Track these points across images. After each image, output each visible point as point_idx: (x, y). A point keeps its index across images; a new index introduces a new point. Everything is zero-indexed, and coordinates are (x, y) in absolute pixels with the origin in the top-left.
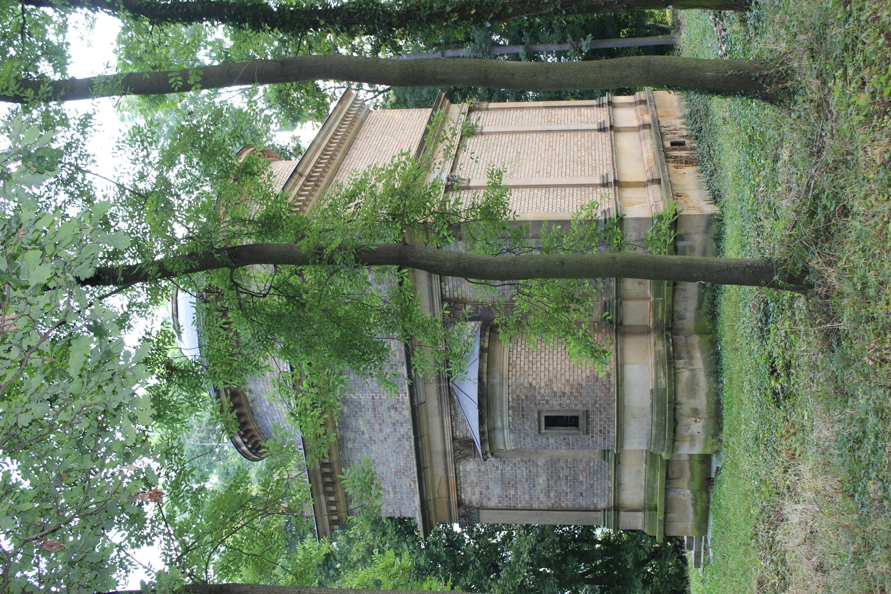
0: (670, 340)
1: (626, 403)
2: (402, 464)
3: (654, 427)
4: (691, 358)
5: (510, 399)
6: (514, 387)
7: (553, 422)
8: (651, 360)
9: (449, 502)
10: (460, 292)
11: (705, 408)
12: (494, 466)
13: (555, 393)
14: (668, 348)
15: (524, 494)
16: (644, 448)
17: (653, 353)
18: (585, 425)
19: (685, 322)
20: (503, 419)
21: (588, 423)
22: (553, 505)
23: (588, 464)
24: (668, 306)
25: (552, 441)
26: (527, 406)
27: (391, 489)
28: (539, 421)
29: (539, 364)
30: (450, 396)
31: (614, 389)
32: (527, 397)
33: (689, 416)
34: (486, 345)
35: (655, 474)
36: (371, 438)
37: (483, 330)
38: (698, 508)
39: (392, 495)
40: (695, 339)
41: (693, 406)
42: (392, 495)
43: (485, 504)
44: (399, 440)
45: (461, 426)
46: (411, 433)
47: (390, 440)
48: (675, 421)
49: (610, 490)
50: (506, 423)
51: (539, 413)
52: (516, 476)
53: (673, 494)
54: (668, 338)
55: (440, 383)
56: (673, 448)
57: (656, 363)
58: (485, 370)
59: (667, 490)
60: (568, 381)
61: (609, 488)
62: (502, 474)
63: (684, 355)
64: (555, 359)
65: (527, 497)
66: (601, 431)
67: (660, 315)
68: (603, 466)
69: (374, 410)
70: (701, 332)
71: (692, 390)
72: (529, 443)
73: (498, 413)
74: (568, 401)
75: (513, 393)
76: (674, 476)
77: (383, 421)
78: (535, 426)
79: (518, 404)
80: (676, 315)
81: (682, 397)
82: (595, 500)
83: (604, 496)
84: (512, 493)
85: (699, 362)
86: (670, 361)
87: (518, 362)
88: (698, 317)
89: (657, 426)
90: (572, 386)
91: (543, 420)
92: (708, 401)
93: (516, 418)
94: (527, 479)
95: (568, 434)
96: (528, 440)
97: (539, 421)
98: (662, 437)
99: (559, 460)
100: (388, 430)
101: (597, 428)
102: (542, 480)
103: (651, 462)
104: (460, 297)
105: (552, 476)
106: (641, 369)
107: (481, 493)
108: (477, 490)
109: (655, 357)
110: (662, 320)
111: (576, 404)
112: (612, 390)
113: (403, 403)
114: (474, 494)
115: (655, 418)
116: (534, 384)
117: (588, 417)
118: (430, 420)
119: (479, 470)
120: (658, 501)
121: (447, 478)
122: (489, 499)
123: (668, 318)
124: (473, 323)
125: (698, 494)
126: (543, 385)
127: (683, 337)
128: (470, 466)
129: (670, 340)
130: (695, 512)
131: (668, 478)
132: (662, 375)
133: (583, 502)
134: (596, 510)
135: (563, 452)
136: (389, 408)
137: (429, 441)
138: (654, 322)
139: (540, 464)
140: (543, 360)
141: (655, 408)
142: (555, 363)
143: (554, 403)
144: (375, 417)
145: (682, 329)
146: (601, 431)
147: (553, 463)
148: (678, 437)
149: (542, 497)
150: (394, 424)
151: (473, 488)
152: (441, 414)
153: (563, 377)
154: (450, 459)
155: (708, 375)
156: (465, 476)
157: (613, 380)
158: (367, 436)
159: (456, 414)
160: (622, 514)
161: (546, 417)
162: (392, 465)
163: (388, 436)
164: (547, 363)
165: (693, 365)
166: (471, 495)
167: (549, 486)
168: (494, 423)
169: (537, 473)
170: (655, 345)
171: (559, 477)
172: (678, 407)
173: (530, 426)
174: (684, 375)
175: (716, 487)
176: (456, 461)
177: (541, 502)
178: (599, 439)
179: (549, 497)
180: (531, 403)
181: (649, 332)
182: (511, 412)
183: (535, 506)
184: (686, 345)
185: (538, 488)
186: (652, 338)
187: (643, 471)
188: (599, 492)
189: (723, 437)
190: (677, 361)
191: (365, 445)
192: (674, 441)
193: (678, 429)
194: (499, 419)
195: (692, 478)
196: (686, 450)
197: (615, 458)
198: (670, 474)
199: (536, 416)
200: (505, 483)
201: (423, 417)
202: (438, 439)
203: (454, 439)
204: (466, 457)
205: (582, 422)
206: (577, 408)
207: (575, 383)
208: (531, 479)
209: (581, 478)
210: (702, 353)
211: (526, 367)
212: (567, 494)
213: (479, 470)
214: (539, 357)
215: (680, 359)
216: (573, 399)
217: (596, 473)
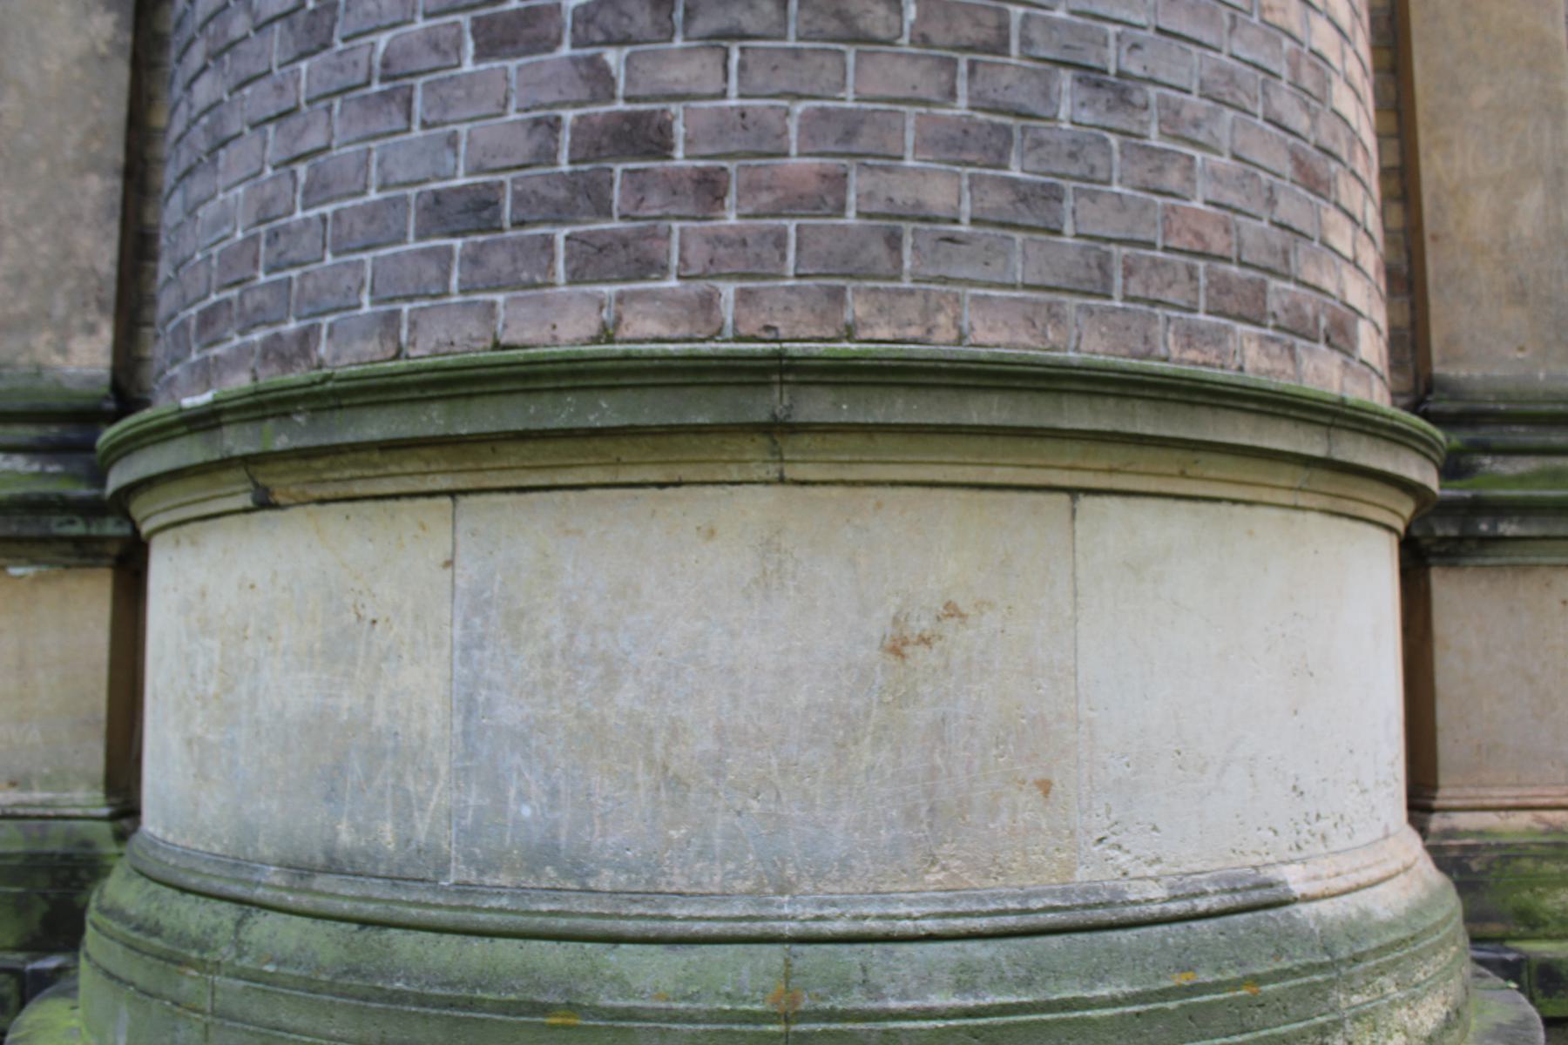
3: (746, 977)
66: (643, 136)
110: (1532, 923)
115: (922, 985)
146: (643, 136)
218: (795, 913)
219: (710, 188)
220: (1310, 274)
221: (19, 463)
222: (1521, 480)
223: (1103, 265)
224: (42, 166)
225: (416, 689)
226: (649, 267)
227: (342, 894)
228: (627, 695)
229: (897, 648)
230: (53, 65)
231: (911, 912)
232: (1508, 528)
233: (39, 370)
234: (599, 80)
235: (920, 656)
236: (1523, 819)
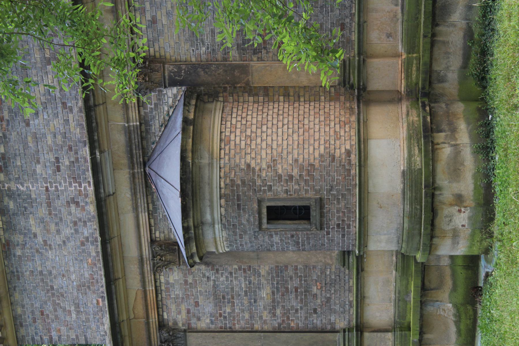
0: (428, 108)
1: (371, 189)
2: (87, 275)
3: (406, 220)
4: (454, 130)
5: (223, 185)
6: (227, 170)
7: (277, 214)
8: (403, 133)
9: (148, 324)
10: (157, 49)
11: (471, 193)
12: (204, 276)
13: (280, 177)
14: (424, 118)
15: (243, 311)
16: (394, 247)
17: (405, 125)
18: (318, 217)
19: (446, 85)
20: (213, 210)
21: (322, 215)
22: (280, 325)
23: (323, 272)
24: (425, 64)
25: (276, 239)
26: (244, 193)
27: (73, 308)
28: (260, 213)
29: (259, 140)
30: (147, 186)
31: (355, 171)
32: (243, 182)
33: (451, 205)
34: (191, 116)
35: (408, 284)
36: (45, 241)
37: (187, 97)
38: (462, 327)
39: (74, 316)
40: (459, 107)
41: (456, 191)
42: (74, 316)
43: (193, 326)
44: (83, 244)
45: (162, 225)
46: (97, 234)
47: (70, 244)
48: (433, 212)
49: (351, 306)
50: (217, 216)
51: (260, 202)
52: (232, 289)
53: (430, 309)
54: (424, 106)
55: (133, 168)
56: (430, 248)
57: (410, 138)
58: (190, 147)
59: (422, 304)
60: (296, 161)
61: (351, 303)
62: (215, 287)
63: (444, 126)
64: (280, 133)
65: (247, 316)
66: (338, 225)
67: (414, 76)
68: (342, 275)
69: (49, 205)
70: (465, 98)
71: (456, 172)
72: (246, 242)
73: (207, 203)
74: (297, 187)
75: (226, 176)
76: (432, 286)
77: (61, 219)
78: (254, 219)
79: (233, 191)
80: (434, 76)
81: (442, 179)
82: (333, 319)
83: (344, 312)
84: (228, 310)
85: (464, 136)
86: (427, 136)
87: (233, 137)
88: (463, 78)
89: (410, 217)
90: (301, 168)
91: (264, 211)
92: (475, 184)
93: (230, 210)
94: (246, 292)
95: (297, 230)
96: (246, 238)
97: (260, 213)
98: (416, 232)
99: (286, 267)
100: (67, 231)
101: (334, 222)
102: (265, 293)
103: (403, 268)
104: (157, 55)
105: (277, 288)
106: (390, 147)
107: (188, 312)
108: (183, 308)
109: (408, 129)
110: (417, 84)
111: (307, 191)
112: (353, 172)
113: (86, 196)
114: (179, 313)
115: (407, 208)
116: (253, 165)
117: (322, 207)
118: (122, 218)
119: (186, 282)
120: (412, 318)
121: (145, 292)
122: (199, 319)
123: (424, 80)
124: (175, 90)
125: (462, 309)
126: (264, 166)
127: (443, 105)
128: (173, 277)
129: (428, 108)
130: (459, 332)
131: (424, 289)
132: (417, 152)
133: (317, 321)
134: (334, 331)
135: (291, 256)
136: (68, 203)
137: (121, 245)
138: (407, 86)
139: (263, 272)
140: (264, 135)
141: (408, 194)
142: (280, 138)
143: (279, 189)
144: (50, 214)
145: (443, 95)
146: (338, 225)
147: (279, 270)
148: (437, 232)
149: (266, 315)
150: (75, 223)
151: (178, 305)
152: (136, 209)
153: (290, 156)
154: (147, 268)
155: (476, 152)
156: (167, 290)
157: (354, 158)
158: (40, 239)
159: (155, 209)
160: (366, 335)
161: (269, 208)
162: (73, 277)
163: (68, 239)
164: (269, 138)
165: (456, 139)
166: (176, 314)
167: (274, 301)
168: (202, 215)
169: (259, 284)
170: (408, 115)
171: (287, 288)
172: (437, 193)
173: (249, 219)
174: (445, 152)
175: (485, 298)
176: (156, 270)
177: (265, 322)
178: (337, 236)
179: (274, 315)
180: (249, 190)
181: (400, 100)
182: (223, 201)
183: (257, 326)
184: (448, 114)
185: (261, 303)
186: (404, 106)
187: (393, 280)
188: (337, 307)
189: (495, 229)
190: (435, 134)
191: (37, 251)
192: (432, 237)
193: (437, 221)
194: (208, 211)
195: (454, 289)
196: (446, 249)
197: (355, 260)
198: (427, 283)
199: (256, 206)
200: (220, 298)
201: (112, 214)
202: (132, 243)
203: (153, 241)
204: (168, 264)
205: (314, 213)
206: (308, 196)
207: (306, 164)
208: (252, 292)
209: (315, 290)
210: (468, 123)
211: (243, 143)
212: (297, 311)
213: (186, 282)
214: (259, 131)
215: (441, 131)
216: (303, 184)
217: (333, 283)
218: (402, 215)
219: (343, 221)
220: (344, 161)
221: (351, 257)
222: (354, 77)
223: (348, 189)
224: (309, 256)
226: (350, 224)
227: (400, 242)
228: (384, 225)
229: (381, 207)
230: (294, 255)
231: (402, 207)
232: (362, 84)
233: (337, 255)
234: (333, 228)
235: (382, 205)
236: (403, 81)
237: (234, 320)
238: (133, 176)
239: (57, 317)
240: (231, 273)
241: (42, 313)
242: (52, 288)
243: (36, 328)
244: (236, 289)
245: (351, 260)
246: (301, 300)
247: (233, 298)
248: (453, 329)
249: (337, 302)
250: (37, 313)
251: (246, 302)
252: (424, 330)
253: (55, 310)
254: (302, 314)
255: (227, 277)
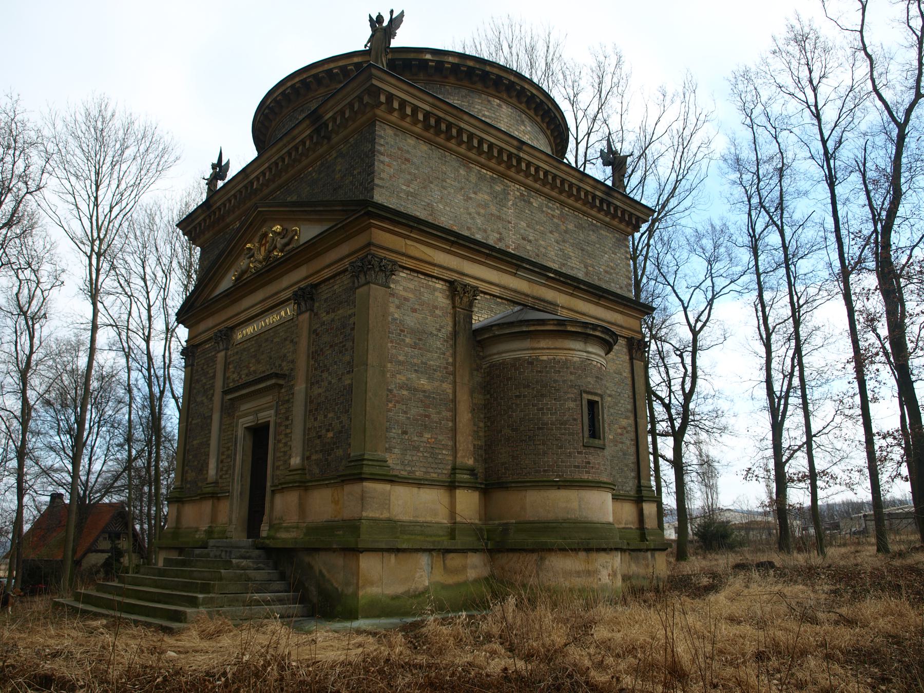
9: (403, 255)
39: (404, 187)
49: (410, 472)
61: (414, 472)
65: (401, 358)
66: (589, 463)
68: (441, 466)
82: (396, 451)
83: (402, 463)
84: (408, 340)
94: (425, 363)
105: (428, 397)
114: (405, 289)
149: (401, 379)
154: (455, 276)
158: (473, 196)
167: (415, 390)
176: (451, 284)
177: (393, 376)
179: (401, 388)
188: (408, 457)
198: (451, 555)
209: (427, 435)
212: (405, 413)
225: (575, 505)
237: (396, 343)
238: (527, 295)
239: (401, 171)
240: (444, 354)
241: (406, 159)
242: (431, 183)
243: (392, 146)
244: (429, 355)
245: (465, 476)
246: (417, 420)
247: (420, 349)
248: (400, 589)
249: (414, 458)
250: (408, 156)
251: (415, 361)
252: (400, 555)
253: (410, 173)
254: (402, 417)
255: (440, 349)
